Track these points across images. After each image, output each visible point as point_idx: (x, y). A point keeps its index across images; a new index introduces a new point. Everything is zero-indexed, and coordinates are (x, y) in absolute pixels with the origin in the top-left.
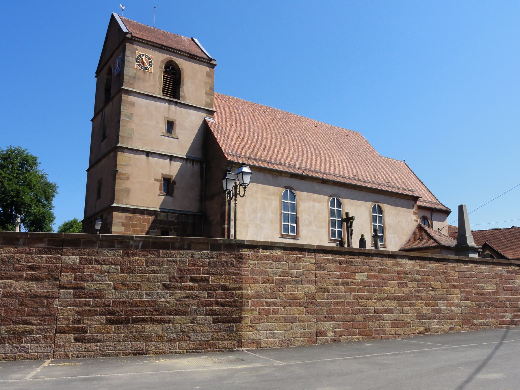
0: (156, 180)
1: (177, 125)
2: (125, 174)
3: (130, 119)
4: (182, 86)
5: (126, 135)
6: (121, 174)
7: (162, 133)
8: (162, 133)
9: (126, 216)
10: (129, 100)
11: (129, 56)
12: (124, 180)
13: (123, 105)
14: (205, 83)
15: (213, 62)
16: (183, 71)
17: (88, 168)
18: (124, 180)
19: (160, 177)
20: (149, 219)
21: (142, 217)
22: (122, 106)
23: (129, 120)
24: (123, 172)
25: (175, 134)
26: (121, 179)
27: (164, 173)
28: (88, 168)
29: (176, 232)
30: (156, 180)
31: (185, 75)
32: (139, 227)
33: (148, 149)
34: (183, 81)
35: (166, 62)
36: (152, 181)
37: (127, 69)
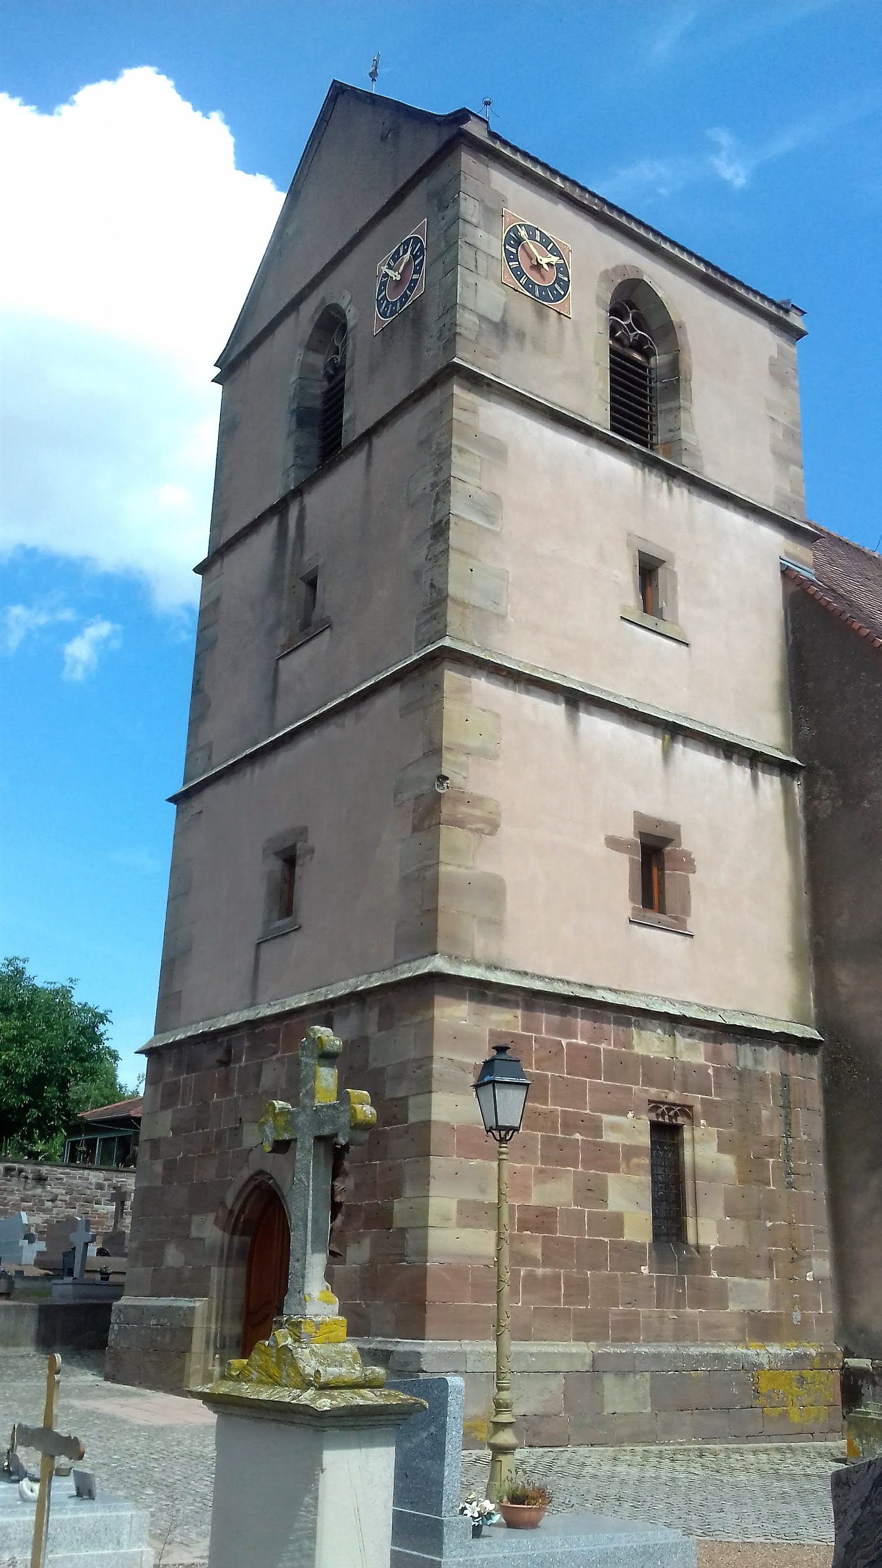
0: (613, 843)
1: (680, 578)
2: (480, 800)
3: (493, 523)
4: (687, 404)
5: (474, 598)
6: (462, 798)
7: (624, 608)
8: (624, 608)
9: (602, 1138)
10: (484, 427)
11: (474, 220)
12: (477, 831)
13: (460, 450)
14: (769, 406)
15: (795, 319)
16: (685, 334)
17: (202, 554)
18: (477, 831)
19: (628, 832)
20: (598, 1050)
21: (564, 1042)
22: (454, 451)
23: (487, 526)
24: (473, 788)
25: (675, 622)
26: (459, 823)
27: (644, 810)
28: (205, 555)
29: (714, 1130)
30: (613, 843)
31: (693, 356)
32: (557, 1099)
33: (575, 680)
34: (688, 381)
35: (620, 281)
36: (598, 848)
37: (471, 279)
